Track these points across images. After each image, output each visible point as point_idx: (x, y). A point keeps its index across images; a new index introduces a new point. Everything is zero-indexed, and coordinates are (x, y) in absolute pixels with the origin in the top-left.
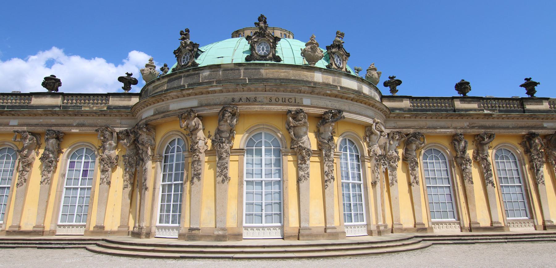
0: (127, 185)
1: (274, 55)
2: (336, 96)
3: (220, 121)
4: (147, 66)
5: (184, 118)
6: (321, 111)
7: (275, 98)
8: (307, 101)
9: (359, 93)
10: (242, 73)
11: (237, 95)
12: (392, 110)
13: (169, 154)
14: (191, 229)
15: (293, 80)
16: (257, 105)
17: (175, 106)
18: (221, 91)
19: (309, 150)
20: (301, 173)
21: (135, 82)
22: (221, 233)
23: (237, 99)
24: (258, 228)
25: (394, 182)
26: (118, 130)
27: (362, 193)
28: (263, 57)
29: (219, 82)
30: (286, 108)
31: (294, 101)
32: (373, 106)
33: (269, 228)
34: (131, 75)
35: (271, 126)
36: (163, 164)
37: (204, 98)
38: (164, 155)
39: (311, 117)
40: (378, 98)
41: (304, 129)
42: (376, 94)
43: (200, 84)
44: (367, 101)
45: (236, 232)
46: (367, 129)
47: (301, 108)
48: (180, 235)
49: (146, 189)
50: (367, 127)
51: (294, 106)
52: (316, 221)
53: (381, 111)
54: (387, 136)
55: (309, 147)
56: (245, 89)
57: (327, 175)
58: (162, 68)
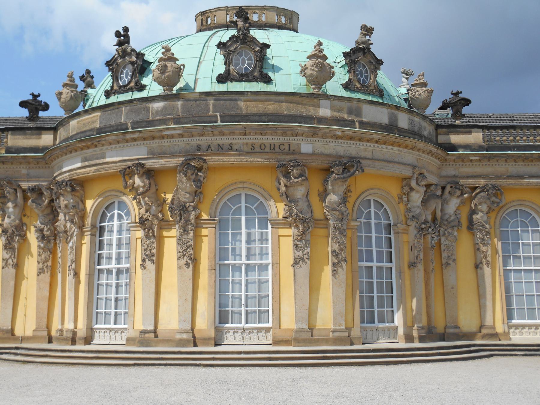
0: (43, 269)
1: (261, 72)
4: (65, 85)
5: (128, 174)
7: (260, 143)
9: (391, 128)
10: (211, 107)
11: (204, 141)
13: (106, 224)
14: (143, 332)
15: (286, 116)
16: (233, 155)
18: (181, 136)
21: (46, 107)
22: (185, 336)
23: (204, 147)
24: (236, 330)
25: (450, 262)
27: (394, 280)
28: (244, 77)
29: (177, 121)
31: (287, 148)
32: (412, 148)
33: (251, 330)
34: (39, 95)
35: (255, 184)
36: (98, 239)
38: (98, 225)
40: (428, 130)
42: (424, 124)
43: (150, 123)
44: (401, 141)
46: (404, 183)
48: (128, 340)
49: (76, 274)
50: (405, 179)
51: (287, 154)
53: (428, 153)
54: (439, 193)
55: (308, 216)
56: (216, 132)
57: (335, 256)
58: (83, 76)
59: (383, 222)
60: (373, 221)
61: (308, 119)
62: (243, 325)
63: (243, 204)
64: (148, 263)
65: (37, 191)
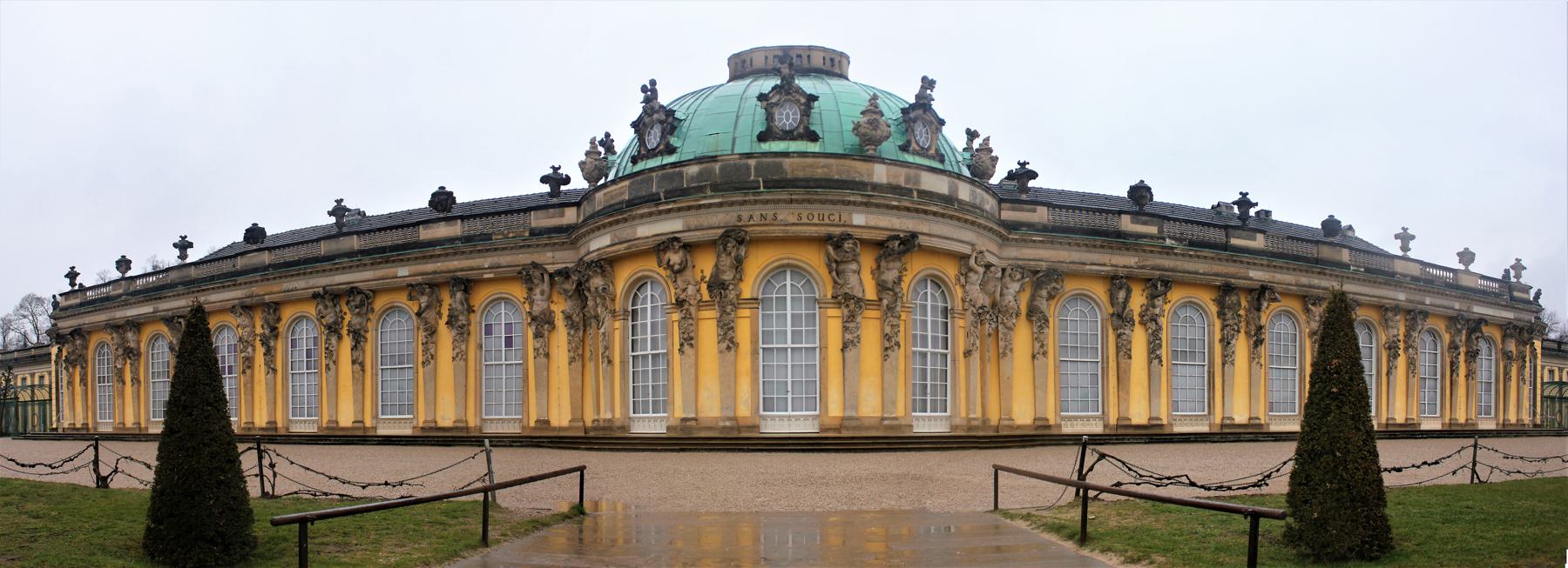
2: (908, 209)
3: (718, 256)
6: (882, 236)
8: (859, 219)
9: (949, 199)
12: (1013, 226)
17: (648, 230)
19: (860, 300)
20: (848, 336)
24: (781, 418)
26: (551, 269)
29: (716, 188)
30: (824, 231)
32: (973, 223)
33: (797, 418)
37: (694, 219)
39: (865, 243)
41: (854, 266)
43: (685, 192)
45: (749, 423)
47: (849, 230)
52: (870, 407)
57: (889, 340)
59: (940, 304)
60: (929, 303)
61: (858, 186)
62: (790, 413)
63: (788, 282)
64: (686, 347)
65: (565, 274)
